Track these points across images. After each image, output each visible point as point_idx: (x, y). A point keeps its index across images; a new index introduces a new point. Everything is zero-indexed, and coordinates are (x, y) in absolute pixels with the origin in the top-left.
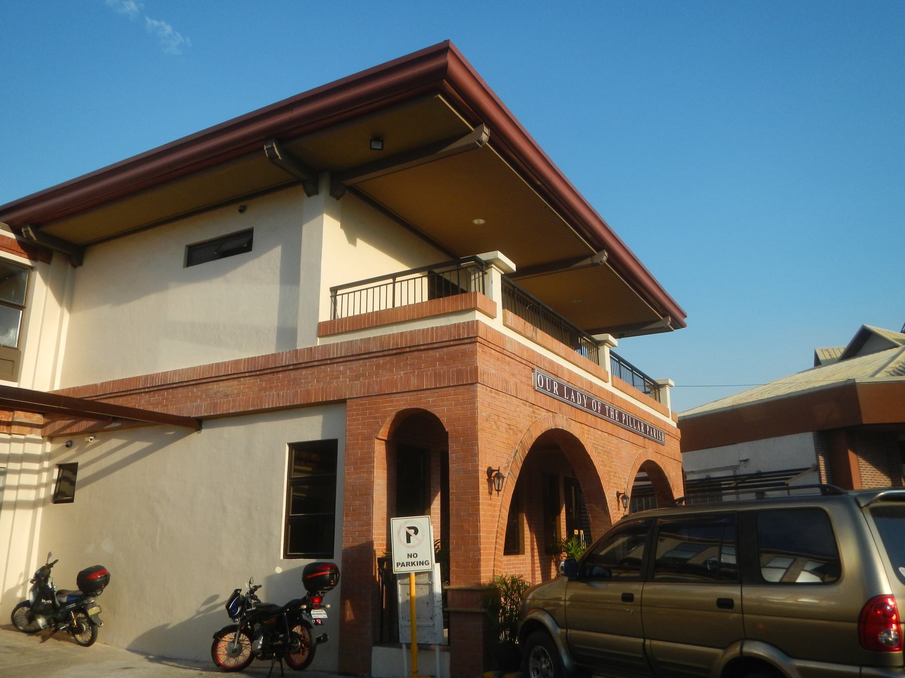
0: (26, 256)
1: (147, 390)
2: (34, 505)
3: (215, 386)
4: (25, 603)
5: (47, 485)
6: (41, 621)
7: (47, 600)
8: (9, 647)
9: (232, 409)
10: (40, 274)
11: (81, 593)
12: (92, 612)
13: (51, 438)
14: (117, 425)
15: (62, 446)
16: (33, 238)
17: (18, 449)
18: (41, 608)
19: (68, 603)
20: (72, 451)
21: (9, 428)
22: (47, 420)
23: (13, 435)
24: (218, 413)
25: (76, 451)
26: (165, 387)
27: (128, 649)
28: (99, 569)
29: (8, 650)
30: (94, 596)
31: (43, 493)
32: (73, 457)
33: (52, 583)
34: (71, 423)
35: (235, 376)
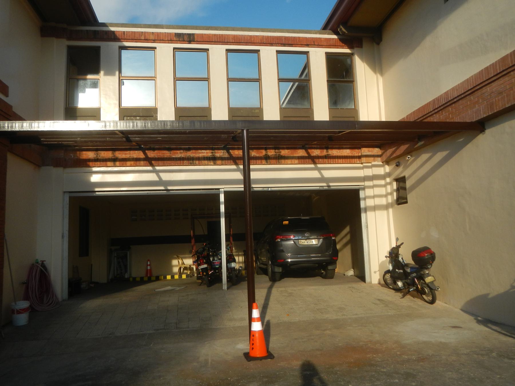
0: (347, 47)
1: (436, 111)
2: (386, 207)
3: (488, 89)
4: (388, 272)
5: (391, 194)
6: (400, 284)
7: (399, 270)
8: (379, 300)
9: (508, 103)
10: (358, 56)
11: (417, 266)
12: (428, 280)
13: (387, 162)
14: (422, 143)
15: (395, 167)
16: (345, 32)
17: (369, 172)
18: (396, 275)
19: (411, 273)
20: (400, 169)
21: (360, 159)
22: (383, 151)
23: (364, 164)
24: (496, 111)
25: (403, 168)
26: (448, 104)
27: (462, 310)
28: (426, 249)
29: (378, 302)
30: (427, 269)
31: (390, 199)
32: (402, 172)
33: (402, 258)
34: (395, 149)
35: (505, 72)
